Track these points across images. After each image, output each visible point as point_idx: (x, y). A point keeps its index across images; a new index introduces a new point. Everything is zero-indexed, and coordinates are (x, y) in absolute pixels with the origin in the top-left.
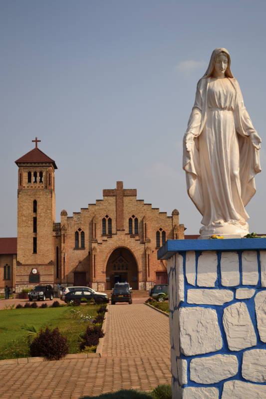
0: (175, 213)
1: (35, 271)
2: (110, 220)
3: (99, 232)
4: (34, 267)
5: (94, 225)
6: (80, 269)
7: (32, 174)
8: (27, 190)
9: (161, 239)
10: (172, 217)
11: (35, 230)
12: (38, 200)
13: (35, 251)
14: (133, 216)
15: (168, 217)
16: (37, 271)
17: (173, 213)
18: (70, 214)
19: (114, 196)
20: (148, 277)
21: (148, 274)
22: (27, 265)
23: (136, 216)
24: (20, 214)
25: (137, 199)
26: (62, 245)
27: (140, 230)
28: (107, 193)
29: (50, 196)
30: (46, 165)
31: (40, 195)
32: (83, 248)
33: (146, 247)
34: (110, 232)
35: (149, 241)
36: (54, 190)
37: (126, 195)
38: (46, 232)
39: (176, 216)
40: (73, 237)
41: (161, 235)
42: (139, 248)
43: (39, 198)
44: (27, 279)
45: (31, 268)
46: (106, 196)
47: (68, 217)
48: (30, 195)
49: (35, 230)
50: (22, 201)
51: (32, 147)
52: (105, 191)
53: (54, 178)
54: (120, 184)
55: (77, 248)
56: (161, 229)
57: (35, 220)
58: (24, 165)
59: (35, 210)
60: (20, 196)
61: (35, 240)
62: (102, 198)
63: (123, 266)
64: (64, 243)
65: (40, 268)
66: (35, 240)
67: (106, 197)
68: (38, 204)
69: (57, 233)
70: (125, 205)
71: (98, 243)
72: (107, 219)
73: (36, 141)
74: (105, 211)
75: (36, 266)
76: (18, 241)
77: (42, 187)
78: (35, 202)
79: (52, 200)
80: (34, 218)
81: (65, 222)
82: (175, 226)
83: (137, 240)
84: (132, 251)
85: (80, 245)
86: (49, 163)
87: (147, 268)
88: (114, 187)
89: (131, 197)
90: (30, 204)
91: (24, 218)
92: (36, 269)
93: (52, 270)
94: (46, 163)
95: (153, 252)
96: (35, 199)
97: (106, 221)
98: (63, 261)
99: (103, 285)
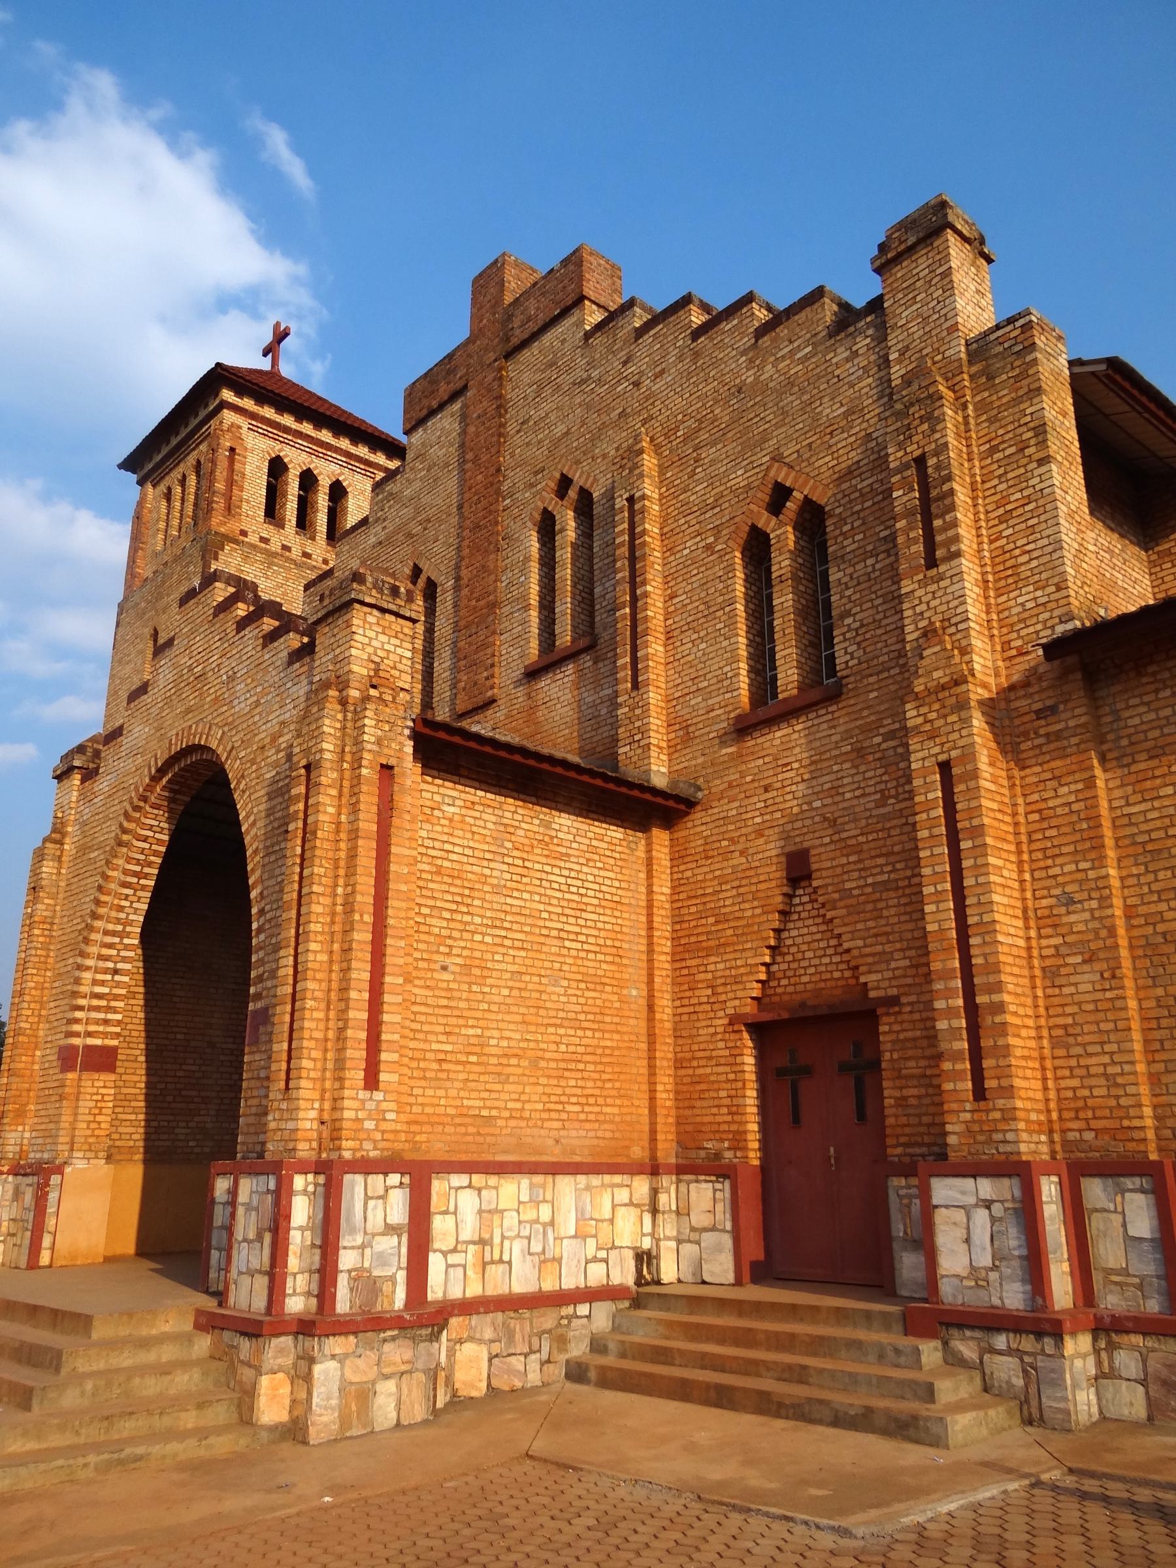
9: (784, 600)
10: (876, 305)
17: (883, 248)
19: (454, 396)
23: (579, 479)
37: (515, 341)
39: (921, 264)
46: (421, 422)
70: (511, 428)
74: (410, 535)
84: (233, 769)
89: (548, 338)
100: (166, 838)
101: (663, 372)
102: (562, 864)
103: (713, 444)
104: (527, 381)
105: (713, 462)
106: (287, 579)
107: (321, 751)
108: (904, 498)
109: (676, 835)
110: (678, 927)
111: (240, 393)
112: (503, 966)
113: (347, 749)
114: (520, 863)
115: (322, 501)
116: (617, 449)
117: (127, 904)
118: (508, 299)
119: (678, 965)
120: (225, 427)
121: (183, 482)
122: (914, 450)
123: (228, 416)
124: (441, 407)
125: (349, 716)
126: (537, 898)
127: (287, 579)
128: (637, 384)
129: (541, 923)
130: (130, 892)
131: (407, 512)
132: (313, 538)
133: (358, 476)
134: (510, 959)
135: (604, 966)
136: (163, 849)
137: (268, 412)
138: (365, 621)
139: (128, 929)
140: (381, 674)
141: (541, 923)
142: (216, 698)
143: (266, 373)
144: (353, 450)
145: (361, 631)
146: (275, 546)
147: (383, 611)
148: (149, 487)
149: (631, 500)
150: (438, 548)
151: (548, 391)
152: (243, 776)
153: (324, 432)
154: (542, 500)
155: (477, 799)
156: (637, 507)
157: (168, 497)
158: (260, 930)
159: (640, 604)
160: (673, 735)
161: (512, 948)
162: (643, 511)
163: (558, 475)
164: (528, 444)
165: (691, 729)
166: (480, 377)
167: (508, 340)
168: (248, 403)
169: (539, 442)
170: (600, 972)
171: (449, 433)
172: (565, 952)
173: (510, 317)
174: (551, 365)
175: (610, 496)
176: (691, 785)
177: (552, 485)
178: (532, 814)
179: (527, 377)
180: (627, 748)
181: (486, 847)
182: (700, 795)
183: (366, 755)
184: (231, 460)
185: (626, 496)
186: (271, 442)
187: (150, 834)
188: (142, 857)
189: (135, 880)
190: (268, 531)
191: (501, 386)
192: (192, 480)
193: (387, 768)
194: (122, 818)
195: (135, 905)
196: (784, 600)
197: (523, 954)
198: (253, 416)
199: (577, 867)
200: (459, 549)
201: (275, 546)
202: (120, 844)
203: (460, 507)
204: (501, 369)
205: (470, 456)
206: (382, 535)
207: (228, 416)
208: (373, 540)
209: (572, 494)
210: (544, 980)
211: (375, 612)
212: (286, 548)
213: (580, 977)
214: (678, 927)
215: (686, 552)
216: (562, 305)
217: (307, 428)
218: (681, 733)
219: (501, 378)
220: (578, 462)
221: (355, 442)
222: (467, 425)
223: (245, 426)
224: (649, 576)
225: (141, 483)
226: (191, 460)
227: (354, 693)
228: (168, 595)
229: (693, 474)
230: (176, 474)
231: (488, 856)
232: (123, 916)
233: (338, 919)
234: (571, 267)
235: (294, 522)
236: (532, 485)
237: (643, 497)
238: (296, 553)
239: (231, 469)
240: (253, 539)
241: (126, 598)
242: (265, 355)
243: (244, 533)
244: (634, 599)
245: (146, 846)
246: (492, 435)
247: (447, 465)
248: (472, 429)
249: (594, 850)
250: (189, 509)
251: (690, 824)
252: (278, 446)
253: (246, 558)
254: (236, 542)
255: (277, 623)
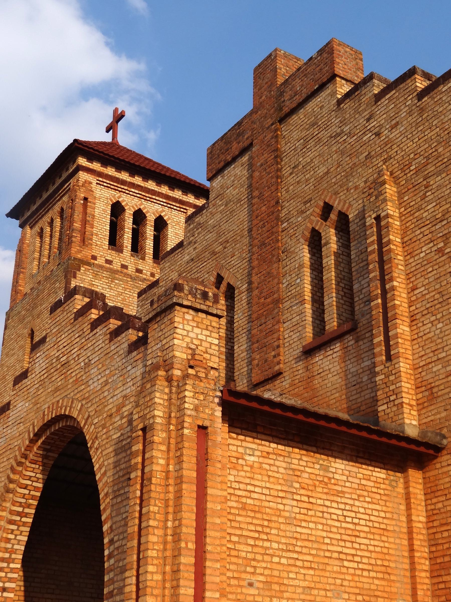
23: (337, 205)
37: (286, 110)
46: (220, 171)
60: (7, 331)
70: (286, 171)
74: (214, 253)
89: (311, 105)
100: (41, 485)
101: (397, 124)
102: (339, 500)
103: (439, 174)
104: (296, 137)
105: (439, 187)
106: (125, 289)
107: (154, 417)
109: (428, 474)
110: (434, 549)
111: (90, 160)
112: (296, 582)
113: (173, 415)
114: (306, 499)
115: (150, 231)
116: (366, 182)
117: (11, 536)
118: (280, 80)
119: (436, 580)
120: (80, 183)
121: (51, 223)
123: (83, 176)
124: (234, 160)
125: (174, 389)
126: (320, 527)
127: (125, 289)
128: (378, 134)
129: (325, 547)
130: (14, 527)
131: (211, 236)
132: (143, 259)
133: (174, 212)
134: (301, 577)
135: (376, 582)
136: (38, 494)
137: (110, 171)
138: (184, 319)
139: (13, 556)
140: (197, 357)
141: (325, 547)
142: (77, 380)
143: (109, 144)
144: (171, 193)
145: (181, 326)
146: (116, 266)
147: (197, 310)
148: (28, 229)
149: (378, 219)
150: (234, 261)
151: (312, 143)
152: (96, 438)
153: (150, 182)
154: (311, 222)
155: (271, 450)
156: (383, 223)
157: (41, 234)
158: (110, 556)
159: (389, 295)
160: (420, 396)
161: (303, 567)
162: (387, 226)
163: (322, 204)
164: (298, 182)
165: (435, 390)
166: (261, 137)
167: (281, 109)
168: (96, 166)
169: (307, 180)
170: (373, 587)
171: (240, 177)
172: (344, 570)
173: (282, 94)
174: (313, 124)
175: (362, 216)
176: (437, 434)
177: (318, 211)
178: (314, 460)
179: (295, 135)
180: (385, 407)
181: (279, 488)
182: (445, 442)
183: (187, 419)
184: (85, 206)
185: (374, 216)
186: (113, 192)
187: (29, 483)
188: (23, 501)
189: (18, 518)
190: (111, 255)
191: (277, 142)
192: (57, 222)
193: (202, 428)
194: (9, 472)
195: (19, 537)
197: (311, 572)
198: (100, 174)
199: (351, 502)
200: (250, 261)
201: (116, 266)
202: (8, 491)
203: (250, 230)
204: (276, 130)
205: (256, 193)
206: (194, 254)
207: (83, 176)
208: (187, 258)
209: (333, 216)
210: (329, 594)
211: (191, 312)
212: (124, 267)
213: (357, 591)
214: (434, 549)
215: (422, 255)
216: (320, 82)
217: (138, 180)
218: (427, 393)
219: (277, 136)
220: (336, 193)
221: (172, 188)
222: (253, 171)
223: (94, 182)
224: (395, 275)
225: (22, 226)
226: (57, 208)
227: (177, 373)
228: (41, 305)
229: (424, 197)
230: (47, 218)
231: (281, 494)
232: (9, 546)
233: (169, 546)
234: (325, 55)
235: (129, 248)
236: (303, 212)
237: (387, 216)
238: (131, 270)
239: (85, 213)
240: (100, 261)
241: (11, 309)
242: (108, 131)
243: (94, 258)
244: (384, 293)
245: (26, 492)
246: (272, 178)
247: (239, 200)
248: (257, 174)
249: (363, 487)
250: (56, 243)
251: (438, 466)
252: (117, 194)
253: (96, 275)
254: (89, 264)
255: (119, 323)
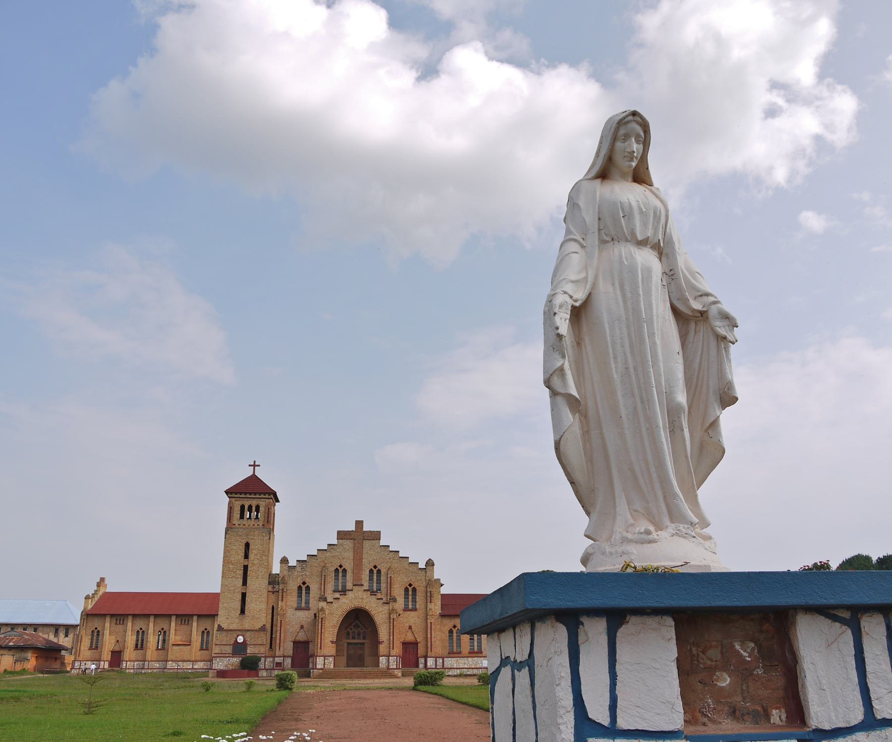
0: (430, 563)
1: (240, 639)
2: (345, 571)
3: (330, 587)
4: (240, 633)
5: (323, 577)
6: (302, 637)
7: (246, 507)
8: (238, 528)
9: (410, 597)
11: (245, 583)
12: (251, 542)
13: (243, 611)
14: (375, 567)
15: (421, 569)
16: (244, 639)
17: (426, 563)
18: (292, 563)
20: (391, 649)
21: (391, 647)
22: (231, 630)
23: (379, 567)
24: (226, 561)
25: (381, 544)
26: (280, 603)
27: (383, 586)
28: (341, 535)
29: (268, 538)
30: (264, 497)
31: (254, 535)
32: (308, 609)
33: (391, 608)
34: (344, 586)
35: (395, 600)
36: (273, 530)
38: (258, 584)
40: (295, 594)
41: (410, 593)
42: (381, 609)
43: (252, 539)
44: (229, 649)
45: (235, 635)
47: (289, 566)
48: (241, 536)
49: (245, 583)
50: (230, 544)
51: (249, 472)
52: (339, 532)
53: (274, 514)
54: (359, 524)
55: (299, 608)
56: (410, 585)
57: (246, 568)
58: (236, 496)
59: (246, 556)
60: (227, 536)
61: (244, 595)
62: (335, 542)
63: (359, 634)
64: (282, 600)
65: (248, 634)
66: (244, 595)
67: (341, 541)
68: (251, 547)
69: (273, 588)
70: (364, 552)
71: (328, 603)
72: (341, 570)
73: (254, 466)
75: (243, 632)
76: (222, 600)
77: (258, 525)
78: (247, 545)
79: (269, 543)
80: (244, 566)
81: (286, 573)
82: (430, 580)
83: (378, 599)
84: (372, 613)
85: (303, 605)
86: (269, 494)
87: (392, 638)
88: (352, 527)
90: (241, 547)
91: (231, 566)
92: (243, 636)
93: (265, 638)
94: (265, 494)
95: (399, 615)
96: (247, 540)
97: (340, 571)
98: (279, 625)
99: (331, 659)
108: (429, 594)
122: (430, 590)
128: (390, 559)
174: (373, 546)
196: (410, 597)
